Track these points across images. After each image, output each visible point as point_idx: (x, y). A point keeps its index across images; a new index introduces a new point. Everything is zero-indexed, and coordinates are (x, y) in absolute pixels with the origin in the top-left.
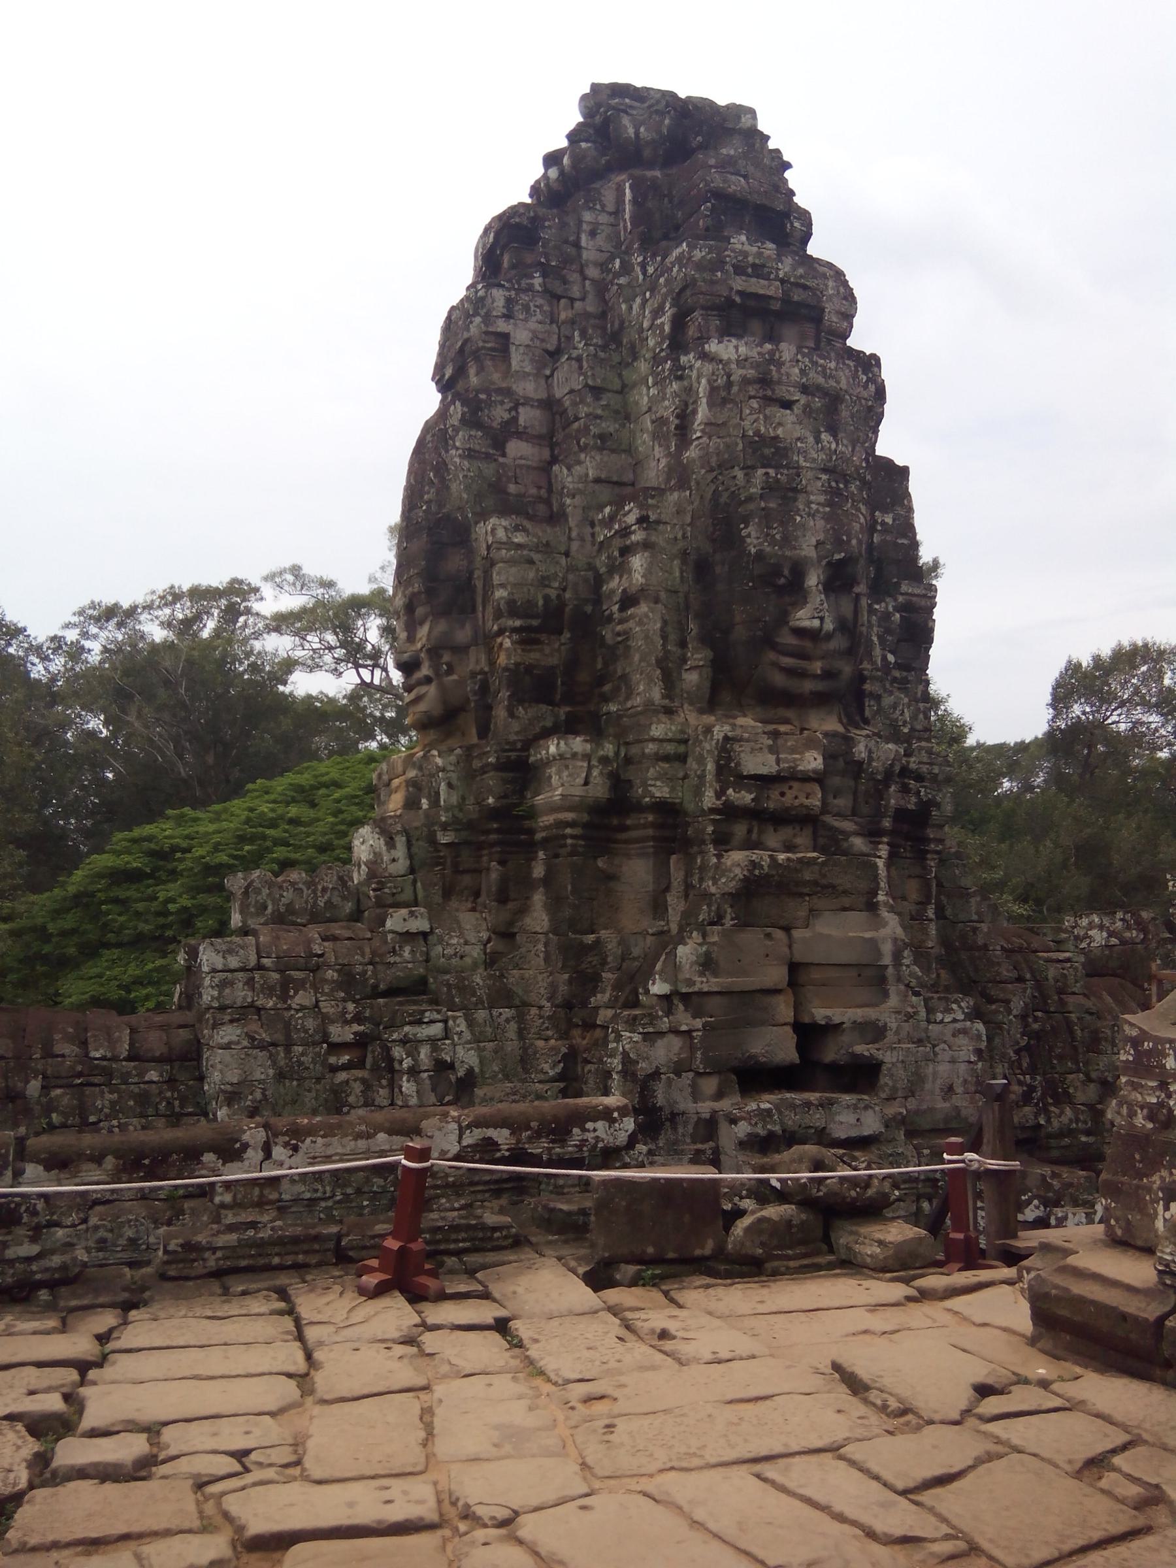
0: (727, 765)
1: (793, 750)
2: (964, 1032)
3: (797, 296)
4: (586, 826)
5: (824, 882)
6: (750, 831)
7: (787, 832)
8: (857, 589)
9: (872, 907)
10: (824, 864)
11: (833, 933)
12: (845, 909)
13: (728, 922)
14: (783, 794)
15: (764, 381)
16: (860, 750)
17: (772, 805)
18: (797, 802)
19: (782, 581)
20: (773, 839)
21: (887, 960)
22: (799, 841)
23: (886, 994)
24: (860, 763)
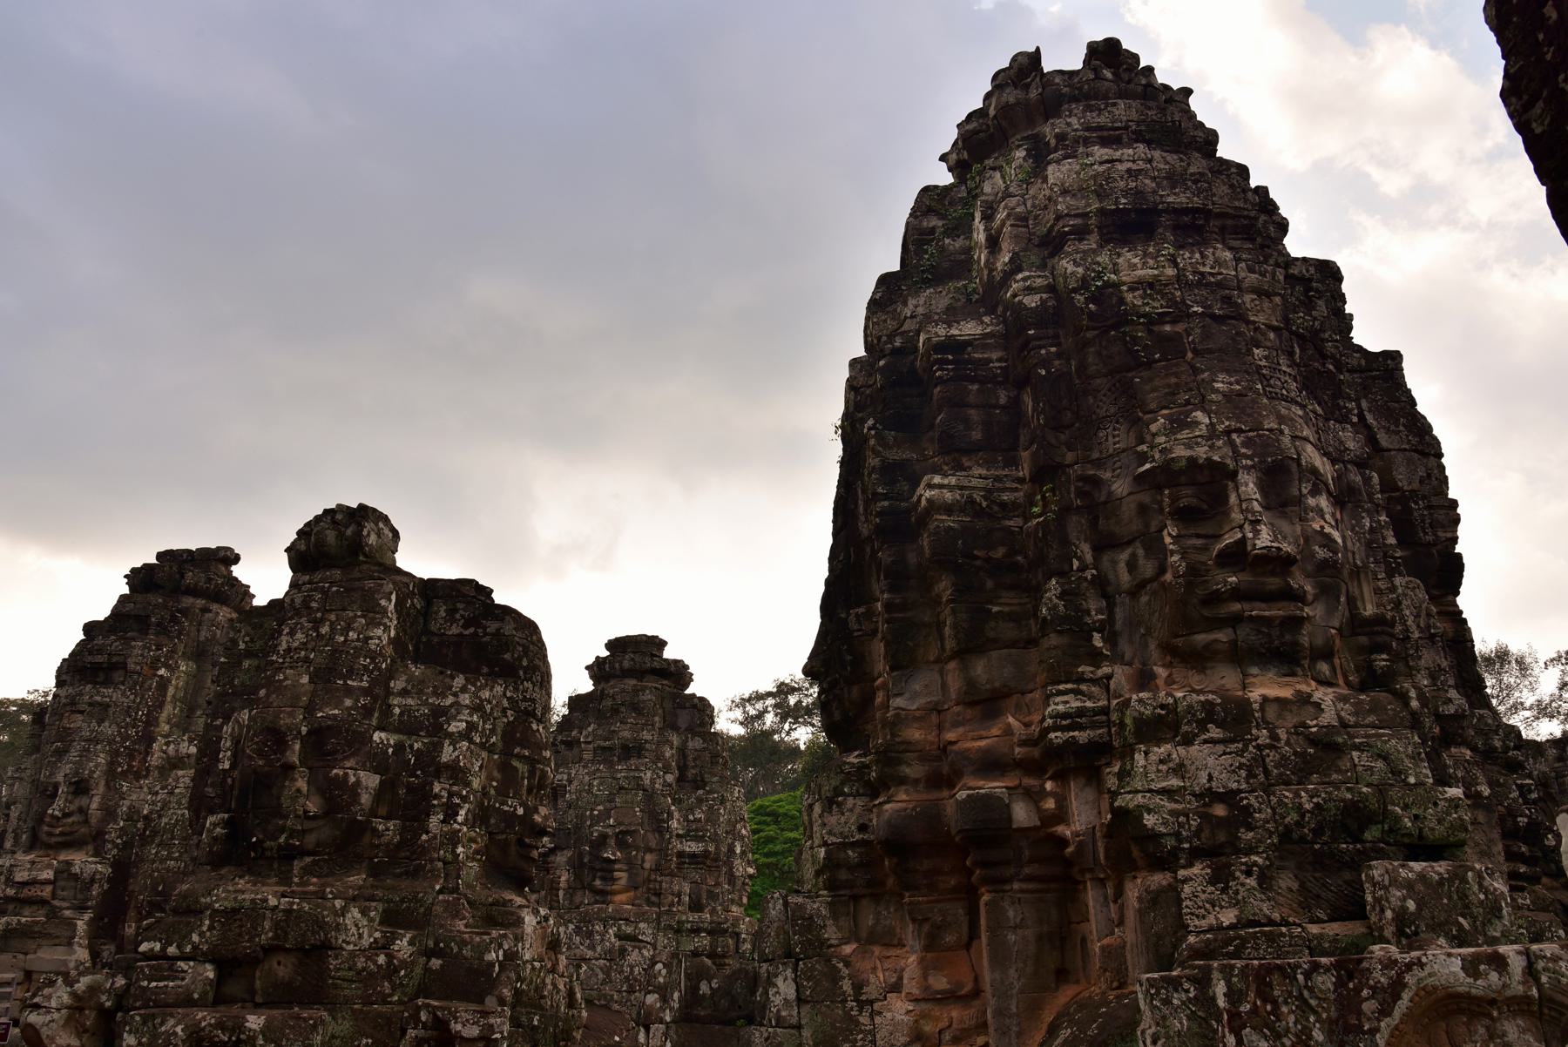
15: (73, 703)
16: (76, 869)
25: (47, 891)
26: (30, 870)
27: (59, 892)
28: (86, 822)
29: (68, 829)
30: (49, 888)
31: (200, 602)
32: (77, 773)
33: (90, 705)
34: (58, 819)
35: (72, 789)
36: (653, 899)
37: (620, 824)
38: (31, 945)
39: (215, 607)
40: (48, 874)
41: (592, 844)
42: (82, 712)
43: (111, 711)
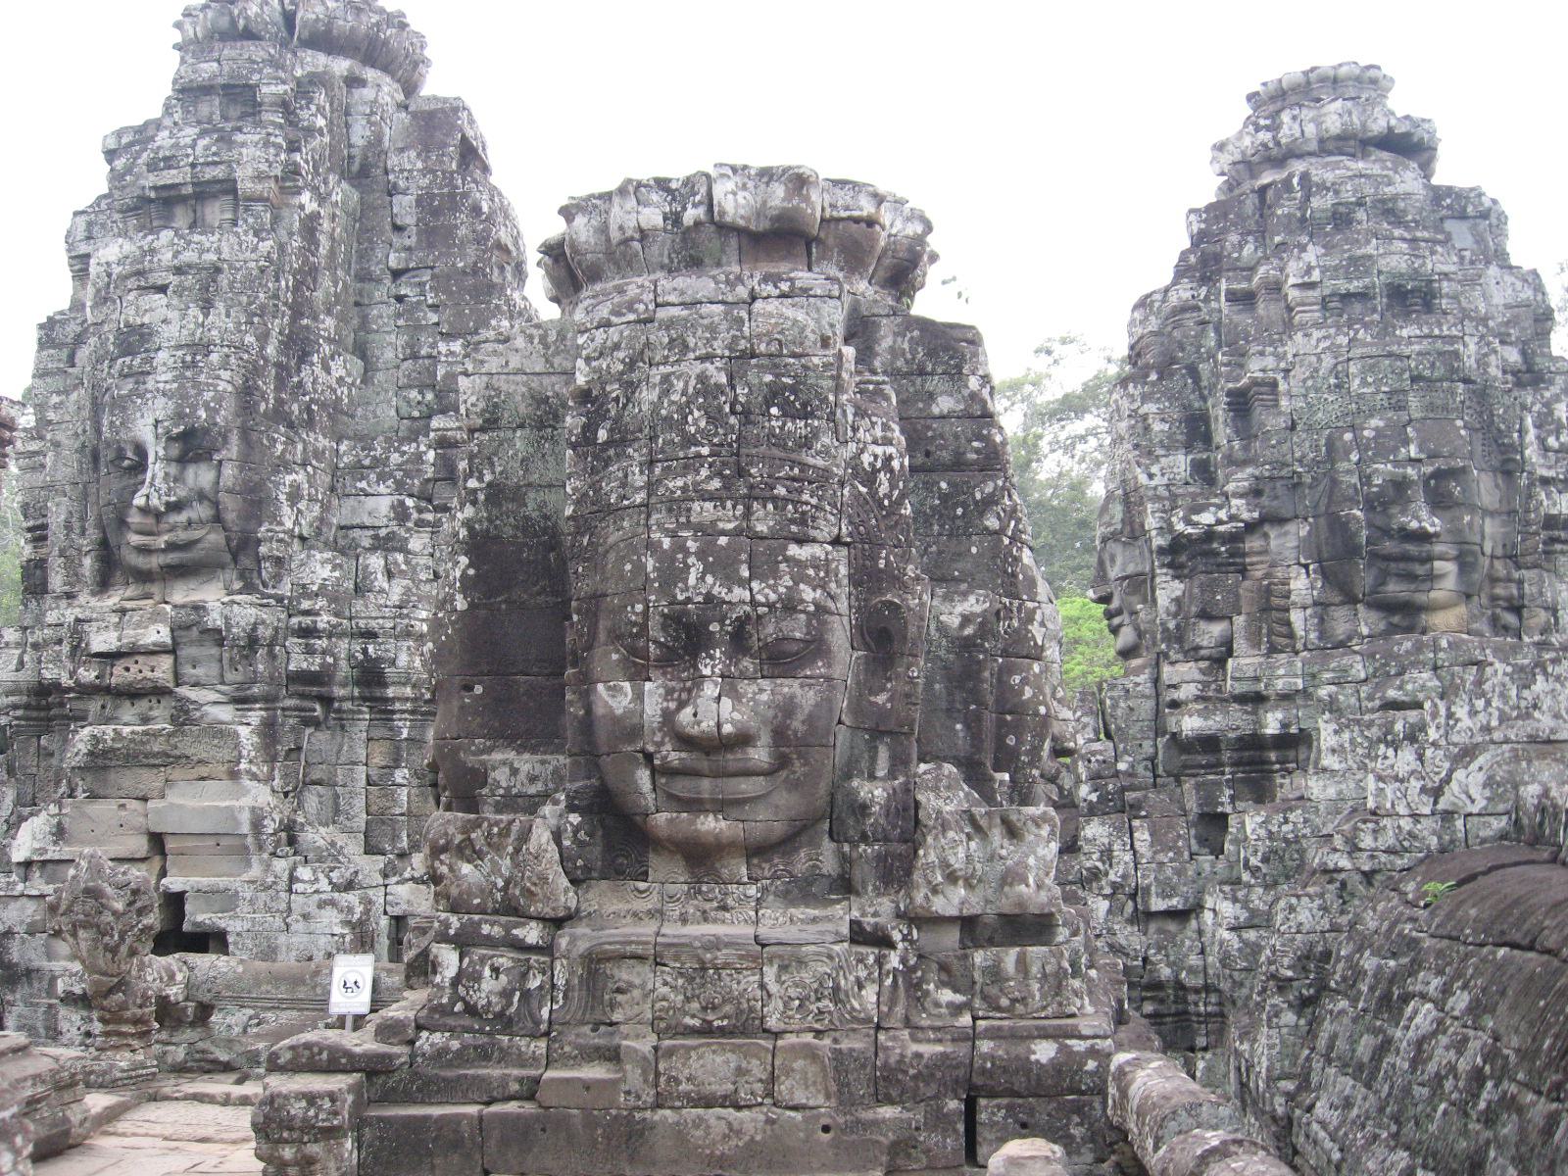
0: (78, 646)
1: (138, 625)
2: (332, 903)
3: (210, 173)
4: (27, 707)
5: (177, 752)
6: (103, 707)
7: (143, 705)
8: (216, 457)
9: (234, 775)
10: (170, 735)
11: (190, 804)
12: (203, 779)
13: (81, 795)
14: (127, 669)
16: (215, 619)
17: (113, 681)
18: (140, 677)
19: (126, 463)
20: (128, 712)
21: (246, 829)
22: (154, 713)
23: (249, 864)
24: (219, 631)
25: (161, 670)
26: (118, 626)
27: (187, 670)
28: (218, 519)
29: (182, 536)
30: (166, 663)
31: (341, 66)
32: (179, 416)
33: (179, 271)
34: (158, 516)
35: (175, 450)
36: (1510, 619)
37: (1433, 456)
38: (150, 780)
39: (370, 74)
40: (157, 634)
41: (1370, 505)
42: (162, 289)
43: (224, 280)
